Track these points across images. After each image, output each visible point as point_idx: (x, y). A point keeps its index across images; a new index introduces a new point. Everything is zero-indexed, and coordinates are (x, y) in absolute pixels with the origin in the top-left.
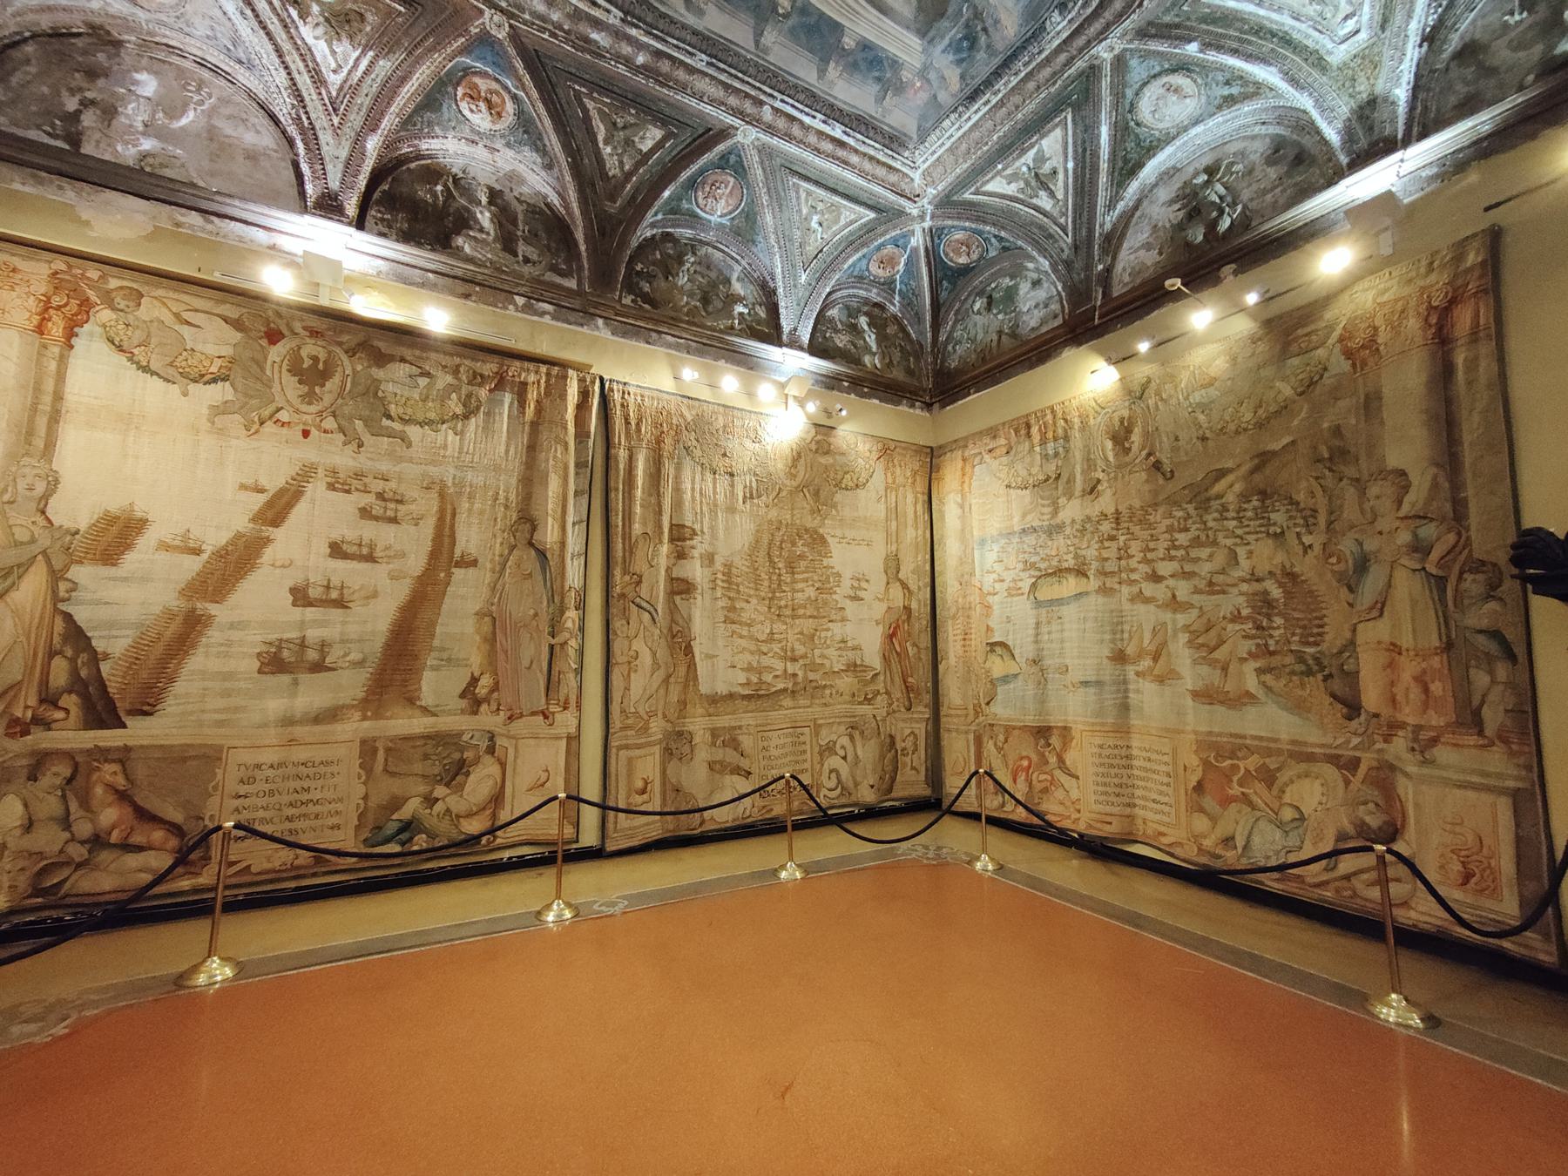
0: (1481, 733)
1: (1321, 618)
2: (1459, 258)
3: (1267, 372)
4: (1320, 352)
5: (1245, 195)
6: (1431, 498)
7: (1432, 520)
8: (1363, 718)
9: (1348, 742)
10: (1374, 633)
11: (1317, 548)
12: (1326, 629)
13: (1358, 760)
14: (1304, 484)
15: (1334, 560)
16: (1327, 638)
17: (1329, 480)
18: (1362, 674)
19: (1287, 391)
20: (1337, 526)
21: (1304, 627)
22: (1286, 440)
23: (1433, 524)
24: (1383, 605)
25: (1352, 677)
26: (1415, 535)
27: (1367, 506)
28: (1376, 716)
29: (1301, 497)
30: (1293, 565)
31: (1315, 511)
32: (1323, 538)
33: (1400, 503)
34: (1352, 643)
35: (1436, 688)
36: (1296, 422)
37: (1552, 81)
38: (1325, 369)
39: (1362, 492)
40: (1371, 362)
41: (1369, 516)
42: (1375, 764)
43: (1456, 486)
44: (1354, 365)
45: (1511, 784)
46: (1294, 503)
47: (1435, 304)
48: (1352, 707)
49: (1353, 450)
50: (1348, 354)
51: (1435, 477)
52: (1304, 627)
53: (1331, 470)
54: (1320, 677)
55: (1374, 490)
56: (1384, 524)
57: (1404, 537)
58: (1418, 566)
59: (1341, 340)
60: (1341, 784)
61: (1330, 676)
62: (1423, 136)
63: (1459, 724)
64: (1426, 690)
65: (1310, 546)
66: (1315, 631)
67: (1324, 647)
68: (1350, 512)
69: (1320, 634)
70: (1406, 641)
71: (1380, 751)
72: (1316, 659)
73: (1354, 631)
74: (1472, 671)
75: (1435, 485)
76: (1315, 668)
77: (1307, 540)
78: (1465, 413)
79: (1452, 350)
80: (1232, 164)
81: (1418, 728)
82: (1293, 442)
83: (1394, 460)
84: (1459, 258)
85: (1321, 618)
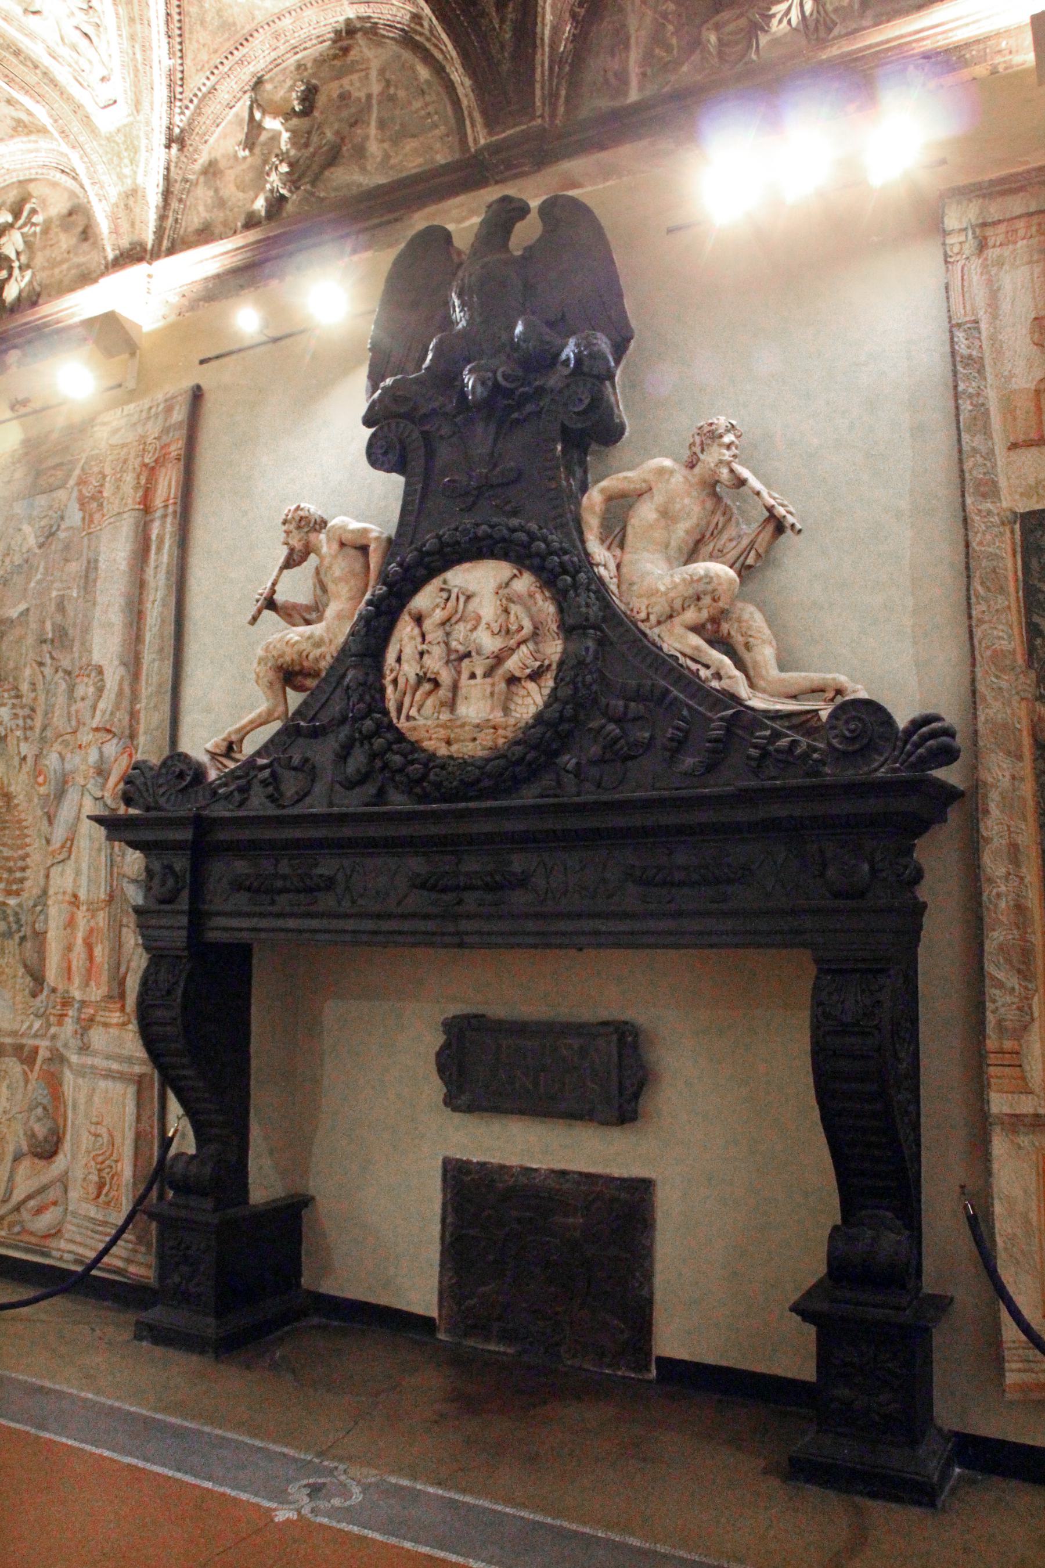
0: (123, 1009)
1: (23, 858)
2: (169, 410)
3: (19, 508)
4: (61, 494)
5: (39, 260)
6: (117, 706)
7: (115, 735)
8: (45, 992)
9: (30, 1027)
10: (63, 880)
11: (30, 761)
12: (28, 871)
13: (35, 1050)
14: (28, 672)
15: (41, 779)
16: (28, 884)
17: (48, 671)
18: (49, 935)
19: (32, 541)
20: (49, 733)
21: (10, 870)
22: (22, 607)
23: (115, 741)
24: (72, 840)
25: (40, 937)
26: (101, 753)
27: (73, 708)
28: (54, 990)
29: (25, 687)
30: (9, 785)
31: (33, 710)
32: (35, 751)
33: (94, 708)
34: (45, 892)
35: (98, 951)
36: (32, 584)
37: (252, 236)
38: (62, 518)
39: (71, 689)
40: (97, 517)
41: (74, 723)
42: (48, 1054)
43: (135, 697)
44: (84, 518)
45: (137, 1069)
46: (18, 697)
47: (147, 461)
48: (38, 978)
49: (71, 631)
50: (82, 505)
51: (122, 679)
52: (10, 870)
53: (52, 658)
54: (17, 937)
55: (80, 691)
56: (85, 737)
57: (93, 756)
58: (99, 794)
59: (81, 482)
60: (22, 1084)
61: (23, 939)
62: (171, 251)
63: (109, 997)
64: (91, 957)
65: (24, 758)
66: (18, 875)
67: (25, 895)
68: (58, 721)
69: (22, 881)
70: (83, 895)
71: (54, 1037)
72: (16, 914)
73: (47, 876)
74: (124, 930)
75: (120, 693)
76: (14, 927)
77: (25, 749)
78: (149, 605)
79: (152, 521)
80: (33, 212)
81: (83, 1003)
82: (28, 610)
83: (97, 658)
84: (169, 410)
85: (23, 858)
